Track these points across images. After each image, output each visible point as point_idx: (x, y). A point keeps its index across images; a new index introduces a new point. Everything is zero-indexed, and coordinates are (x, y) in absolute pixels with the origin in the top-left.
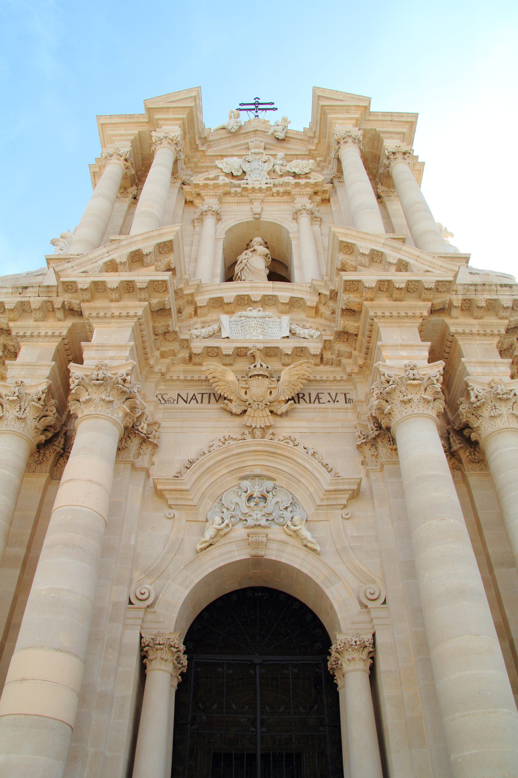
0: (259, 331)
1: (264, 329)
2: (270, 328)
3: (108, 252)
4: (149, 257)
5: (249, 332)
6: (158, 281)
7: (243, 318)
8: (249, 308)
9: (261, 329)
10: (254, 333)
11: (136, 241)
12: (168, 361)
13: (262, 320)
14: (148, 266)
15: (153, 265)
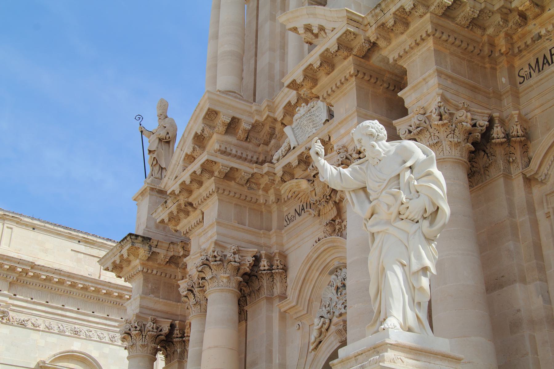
0: (311, 124)
1: (314, 121)
2: (317, 116)
3: (182, 150)
4: (205, 132)
5: (306, 131)
6: (205, 162)
7: (298, 121)
8: (297, 110)
9: (312, 123)
10: (310, 130)
11: (191, 127)
12: (272, 191)
13: (309, 114)
14: (210, 137)
15: (214, 133)
